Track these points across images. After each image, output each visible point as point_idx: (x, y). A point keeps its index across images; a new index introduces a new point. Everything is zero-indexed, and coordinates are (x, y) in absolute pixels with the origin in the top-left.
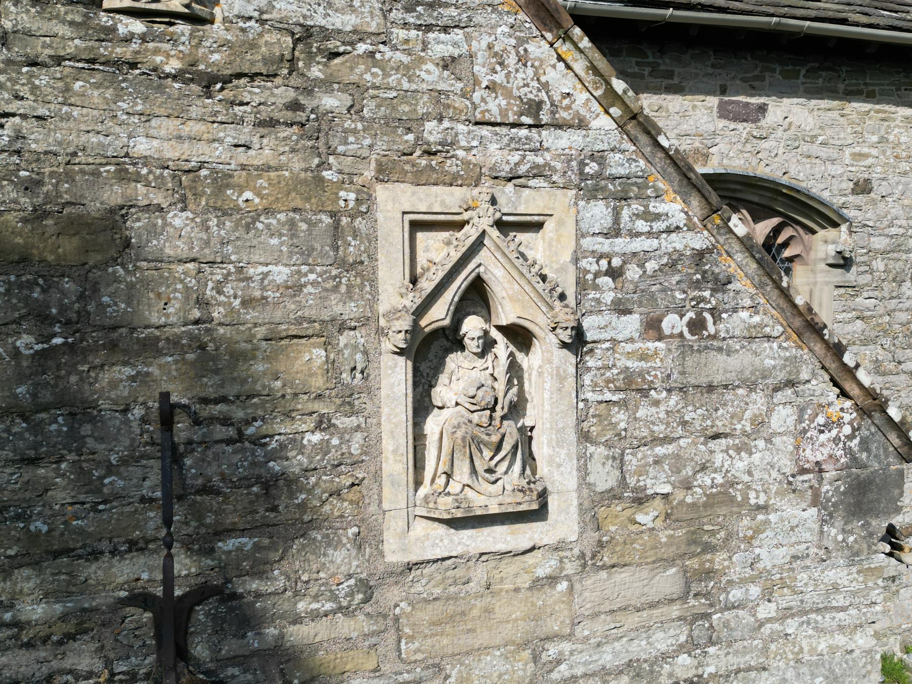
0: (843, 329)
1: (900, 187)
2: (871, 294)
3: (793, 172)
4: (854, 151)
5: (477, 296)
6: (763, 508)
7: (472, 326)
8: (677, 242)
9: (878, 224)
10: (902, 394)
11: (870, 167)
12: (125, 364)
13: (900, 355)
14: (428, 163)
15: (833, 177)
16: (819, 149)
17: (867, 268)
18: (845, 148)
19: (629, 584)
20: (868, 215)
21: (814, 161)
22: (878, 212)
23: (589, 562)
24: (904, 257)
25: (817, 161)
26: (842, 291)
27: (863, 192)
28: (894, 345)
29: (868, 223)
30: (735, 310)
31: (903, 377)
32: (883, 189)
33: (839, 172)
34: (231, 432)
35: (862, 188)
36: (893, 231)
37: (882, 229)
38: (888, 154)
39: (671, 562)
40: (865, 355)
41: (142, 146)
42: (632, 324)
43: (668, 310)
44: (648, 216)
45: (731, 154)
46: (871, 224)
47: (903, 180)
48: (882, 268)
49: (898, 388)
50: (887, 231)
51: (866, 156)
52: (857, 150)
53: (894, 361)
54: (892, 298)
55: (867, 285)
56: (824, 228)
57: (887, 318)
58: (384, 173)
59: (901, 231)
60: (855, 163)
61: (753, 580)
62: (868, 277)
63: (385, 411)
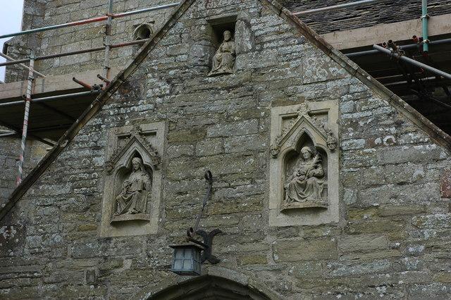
5: (305, 139)
6: (424, 212)
7: (305, 149)
8: (380, 111)
12: (203, 166)
14: (288, 99)
19: (361, 241)
23: (346, 231)
30: (406, 133)
34: (227, 184)
39: (380, 234)
41: (212, 108)
42: (362, 142)
43: (376, 137)
44: (366, 104)
58: (274, 104)
61: (420, 243)
63: (271, 176)
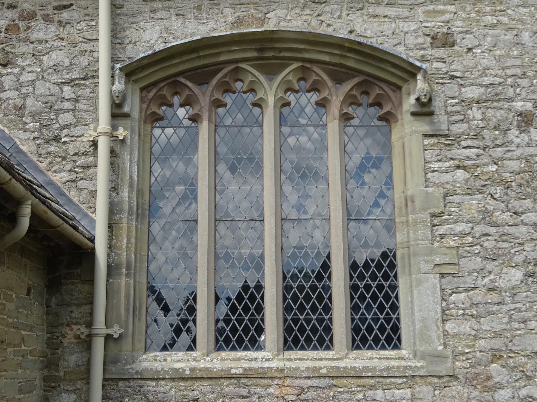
0: (439, 178)
1: (489, 39)
2: (470, 143)
3: (359, 29)
4: (427, 8)
9: (467, 74)
10: (526, 247)
11: (448, 22)
13: (515, 204)
15: (407, 33)
16: (386, 9)
17: (462, 117)
18: (416, 7)
20: (453, 67)
21: (382, 19)
22: (464, 63)
24: (506, 105)
25: (386, 19)
26: (434, 140)
27: (444, 45)
28: (507, 194)
29: (454, 74)
31: (523, 229)
32: (469, 41)
33: (412, 28)
35: (444, 41)
36: (487, 80)
37: (473, 79)
38: (468, 9)
40: (471, 204)
45: (289, 17)
46: (458, 74)
47: (491, 32)
48: (479, 116)
49: (520, 241)
50: (479, 81)
51: (443, 12)
52: (431, 7)
53: (509, 211)
54: (497, 146)
55: (463, 134)
56: (406, 81)
57: (494, 168)
59: (498, 80)
60: (431, 19)
62: (465, 126)
